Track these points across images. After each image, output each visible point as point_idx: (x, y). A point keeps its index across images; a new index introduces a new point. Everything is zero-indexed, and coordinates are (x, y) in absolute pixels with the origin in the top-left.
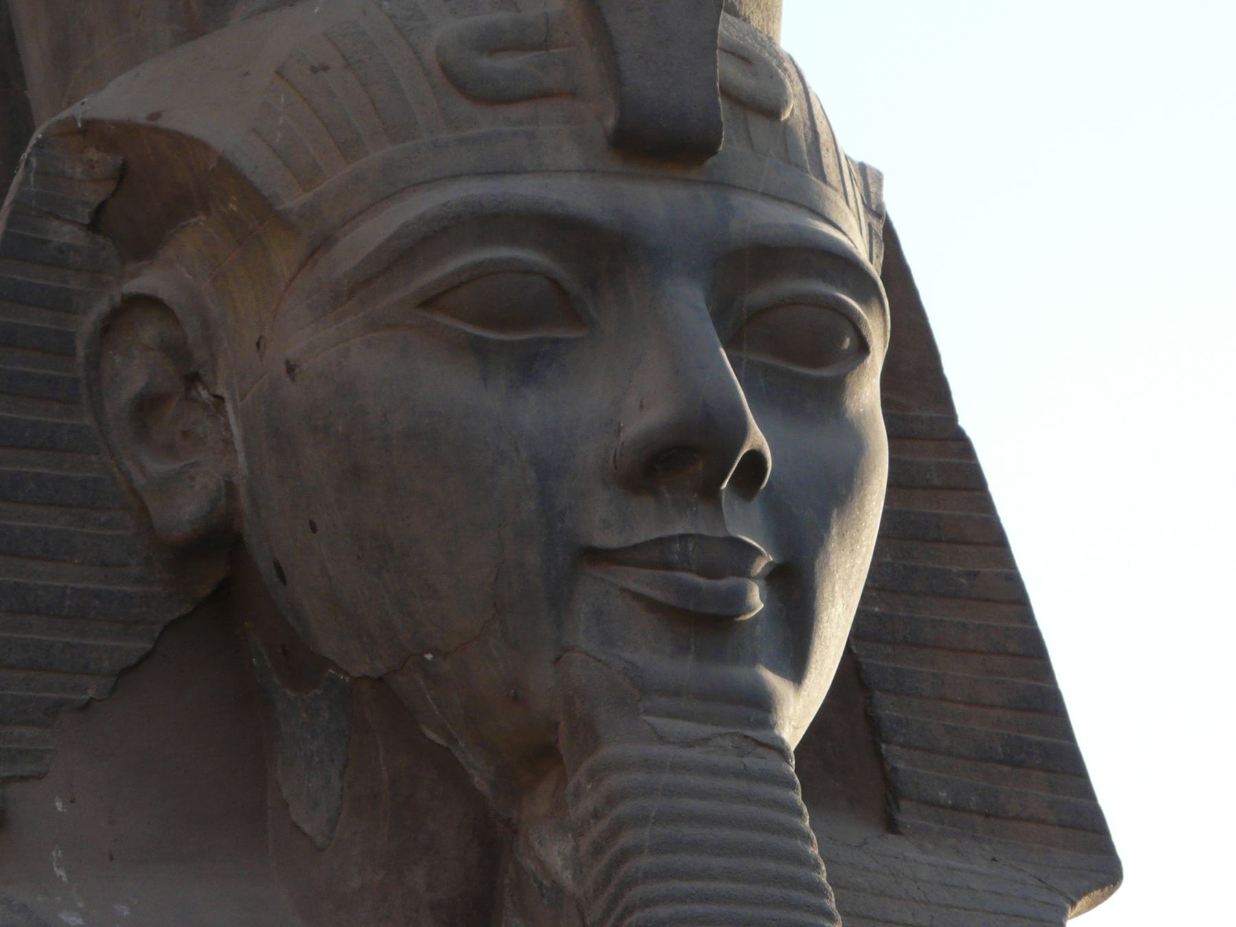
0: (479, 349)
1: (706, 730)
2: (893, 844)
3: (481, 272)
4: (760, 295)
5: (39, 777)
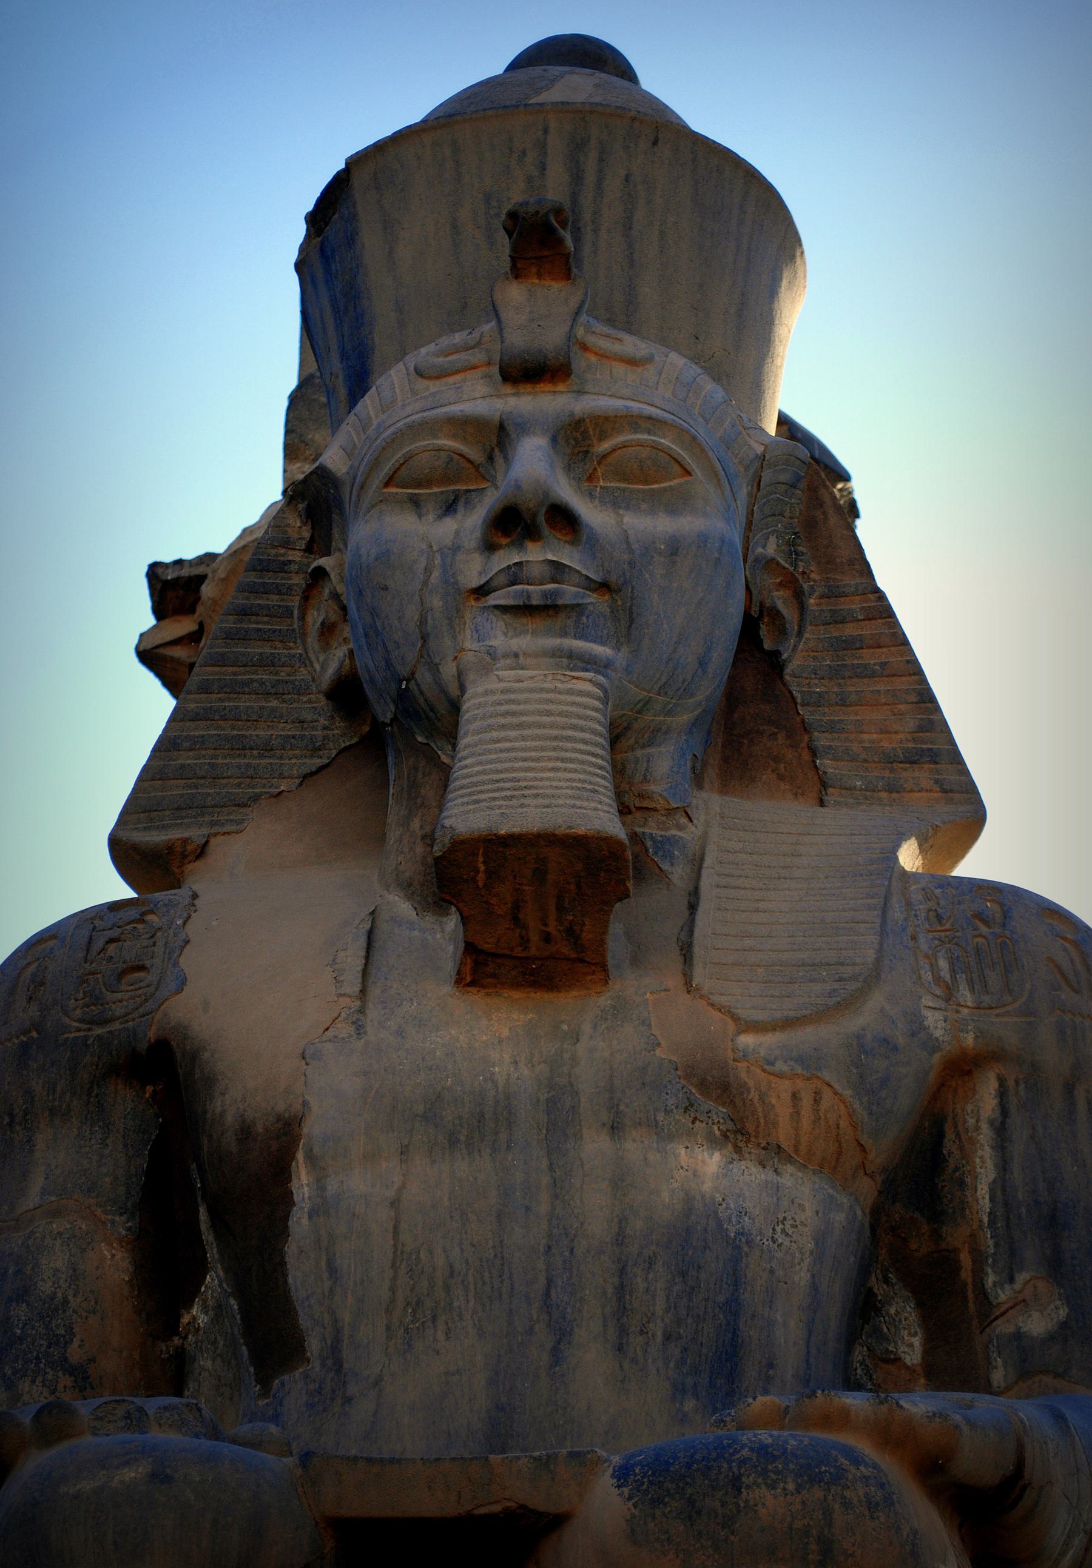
0: (415, 503)
1: (536, 672)
2: (826, 816)
3: (408, 458)
4: (606, 446)
5: (238, 832)
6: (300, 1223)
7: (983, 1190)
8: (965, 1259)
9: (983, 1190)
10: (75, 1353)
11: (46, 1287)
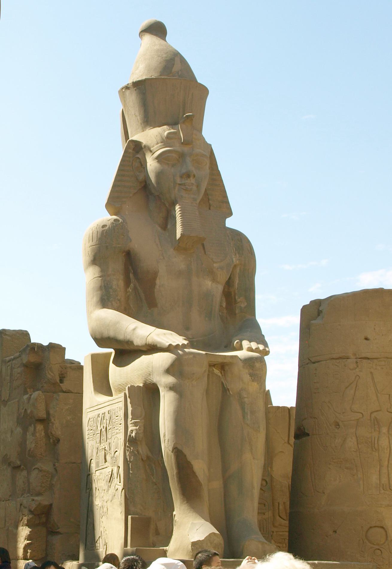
6: (157, 287)
7: (236, 284)
8: (233, 293)
9: (236, 284)
10: (119, 298)
11: (114, 287)
